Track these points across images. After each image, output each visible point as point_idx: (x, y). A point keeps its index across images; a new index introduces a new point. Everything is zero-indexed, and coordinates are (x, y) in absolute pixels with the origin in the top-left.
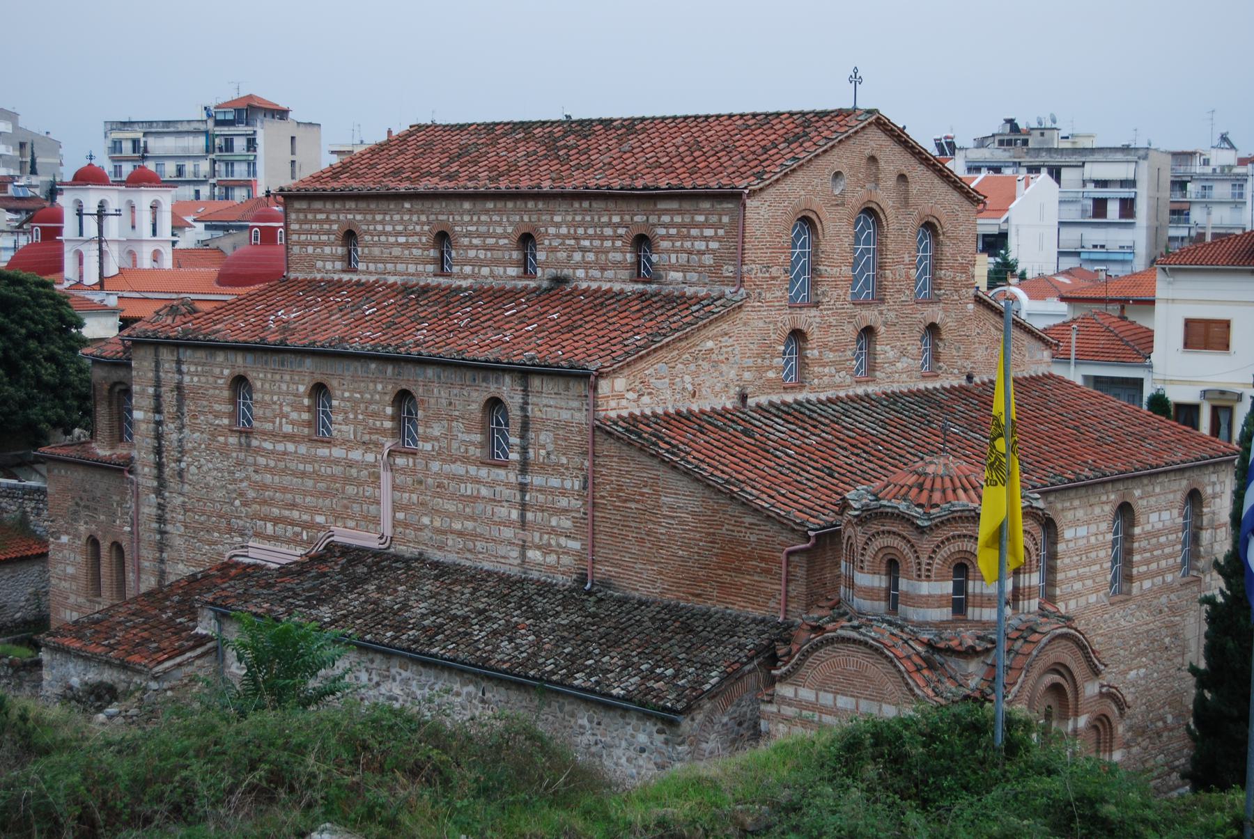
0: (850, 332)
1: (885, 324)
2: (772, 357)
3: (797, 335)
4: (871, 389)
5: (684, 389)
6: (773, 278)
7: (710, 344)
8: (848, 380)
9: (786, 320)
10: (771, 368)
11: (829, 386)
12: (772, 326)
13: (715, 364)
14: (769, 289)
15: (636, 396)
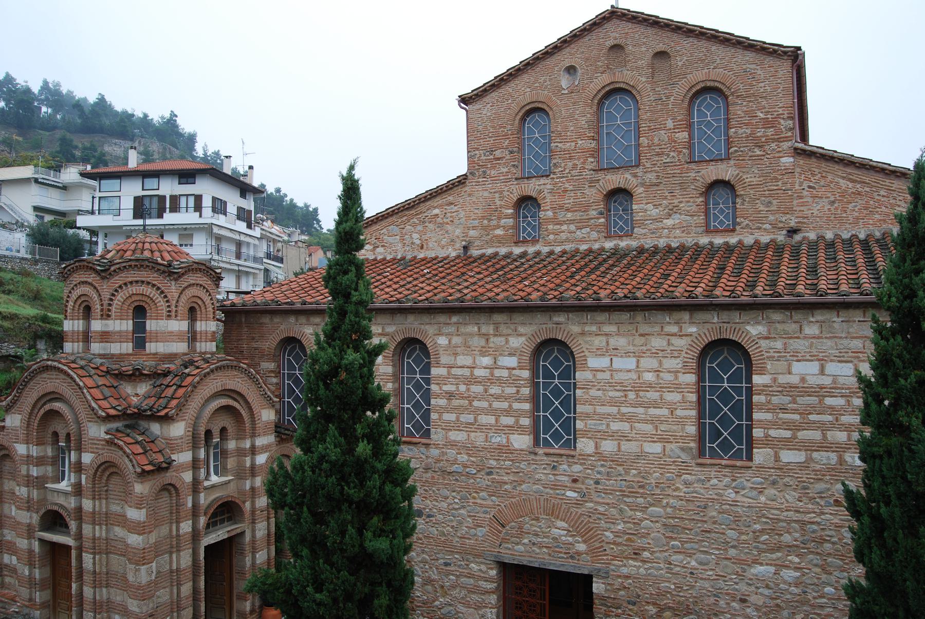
0: (593, 195)
1: (643, 184)
2: (499, 218)
3: (526, 202)
4: (623, 244)
5: (413, 243)
6: (499, 159)
7: (436, 211)
8: (594, 235)
9: (516, 191)
10: (498, 227)
11: (568, 240)
12: (497, 195)
13: (441, 226)
14: (494, 168)
15: (371, 247)
